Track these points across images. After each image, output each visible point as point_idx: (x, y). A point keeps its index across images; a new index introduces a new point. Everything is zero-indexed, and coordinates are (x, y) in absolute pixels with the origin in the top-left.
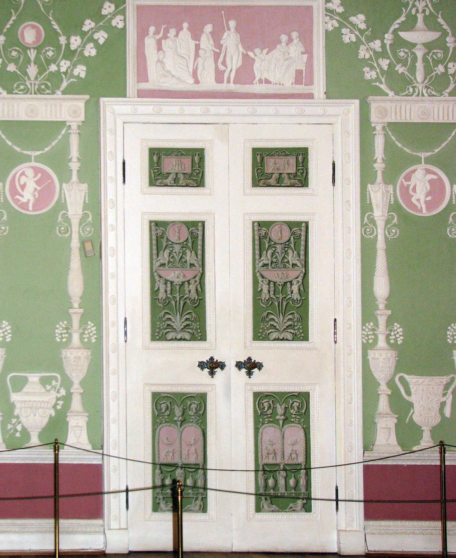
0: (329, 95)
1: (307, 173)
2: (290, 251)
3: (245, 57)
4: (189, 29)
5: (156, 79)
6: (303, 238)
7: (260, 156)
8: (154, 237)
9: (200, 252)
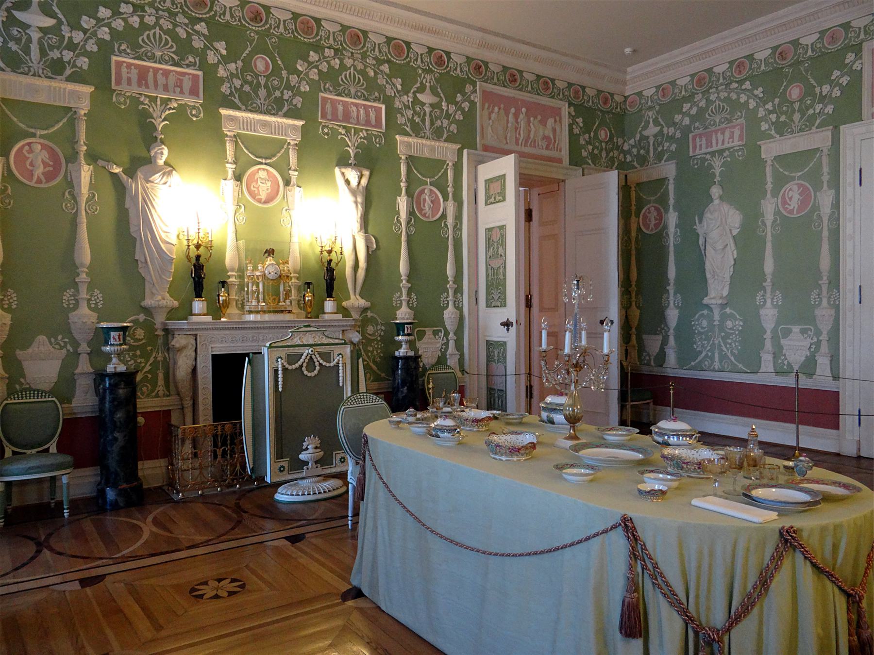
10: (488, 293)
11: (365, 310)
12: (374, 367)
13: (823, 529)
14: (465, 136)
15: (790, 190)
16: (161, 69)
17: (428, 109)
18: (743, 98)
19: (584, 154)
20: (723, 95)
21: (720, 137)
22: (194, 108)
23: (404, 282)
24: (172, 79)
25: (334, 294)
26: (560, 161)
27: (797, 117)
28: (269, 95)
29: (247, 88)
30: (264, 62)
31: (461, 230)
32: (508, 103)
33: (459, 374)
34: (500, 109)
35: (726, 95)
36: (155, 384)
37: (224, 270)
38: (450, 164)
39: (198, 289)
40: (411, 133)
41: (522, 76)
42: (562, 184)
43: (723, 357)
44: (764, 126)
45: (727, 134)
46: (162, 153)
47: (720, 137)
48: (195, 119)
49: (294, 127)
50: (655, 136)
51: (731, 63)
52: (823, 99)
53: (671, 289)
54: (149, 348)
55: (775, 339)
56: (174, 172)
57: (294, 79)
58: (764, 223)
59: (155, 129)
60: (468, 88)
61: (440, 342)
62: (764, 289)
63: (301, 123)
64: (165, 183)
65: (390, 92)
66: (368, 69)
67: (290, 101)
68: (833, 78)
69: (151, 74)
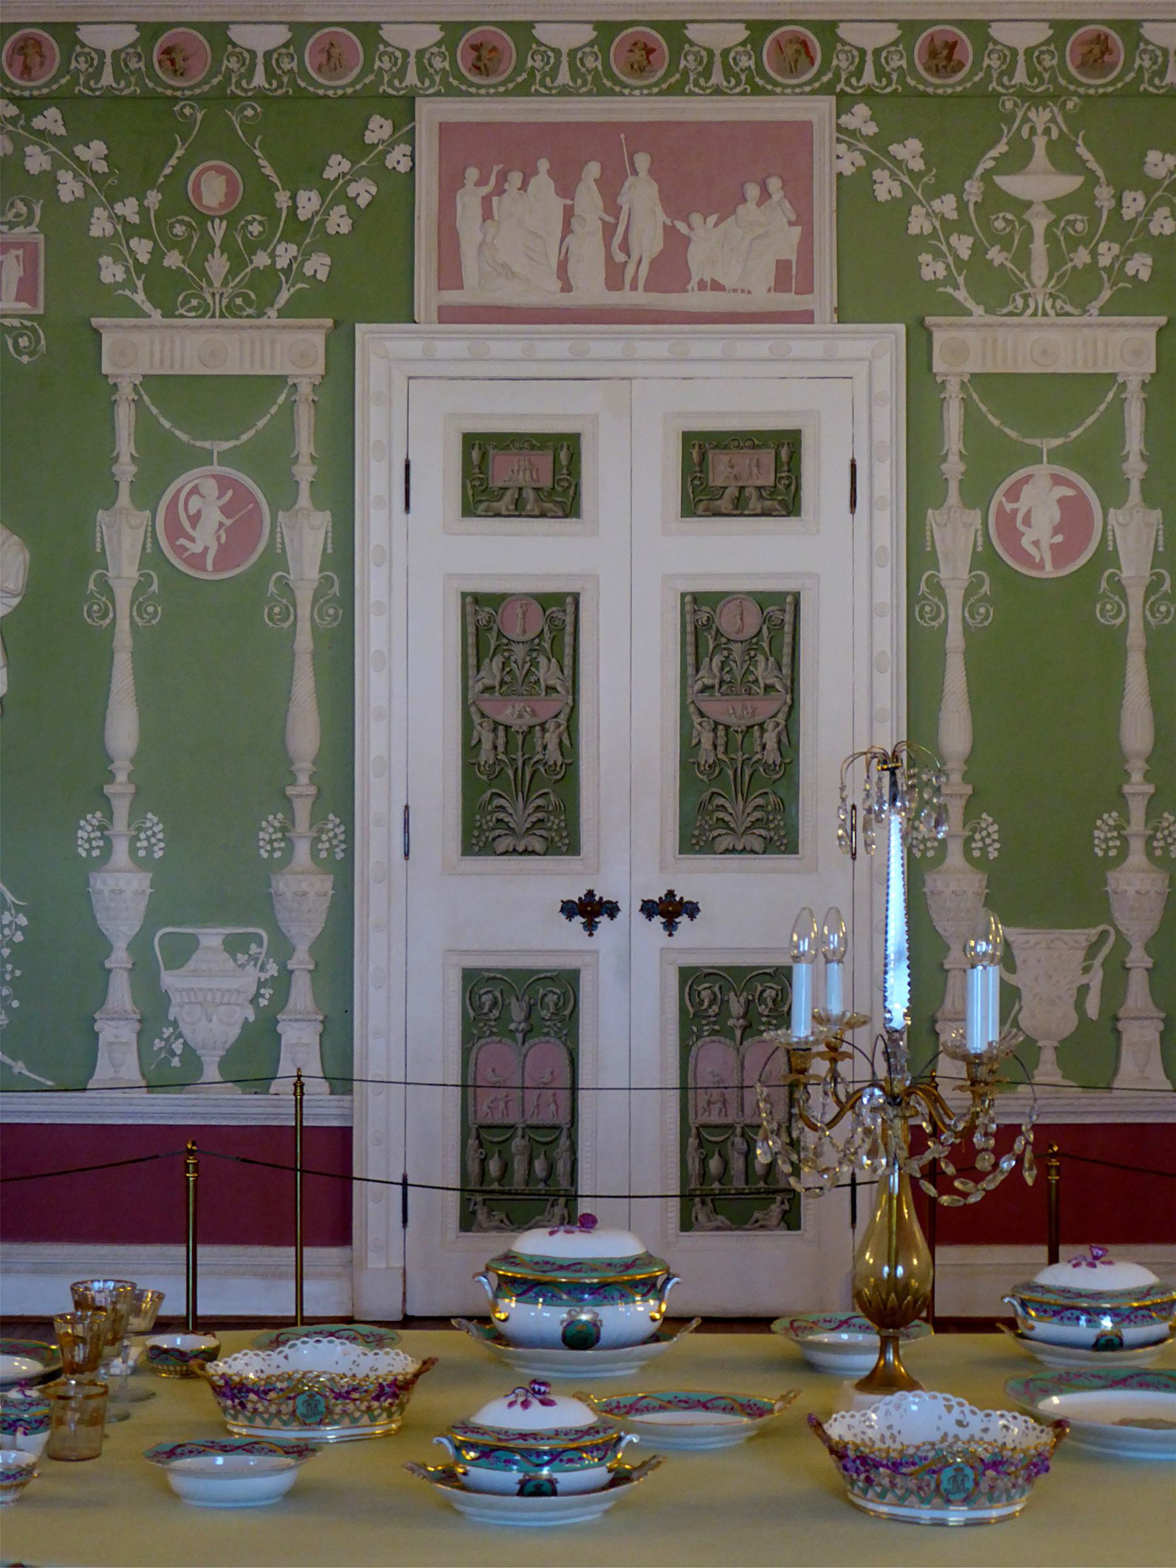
1: (798, 488)
3: (670, 232)
6: (788, 628)
8: (471, 629)
9: (568, 661)
15: (195, 490)
27: (218, 265)
44: (111, 271)
52: (297, 229)
58: (106, 588)
62: (105, 804)
68: (330, 174)
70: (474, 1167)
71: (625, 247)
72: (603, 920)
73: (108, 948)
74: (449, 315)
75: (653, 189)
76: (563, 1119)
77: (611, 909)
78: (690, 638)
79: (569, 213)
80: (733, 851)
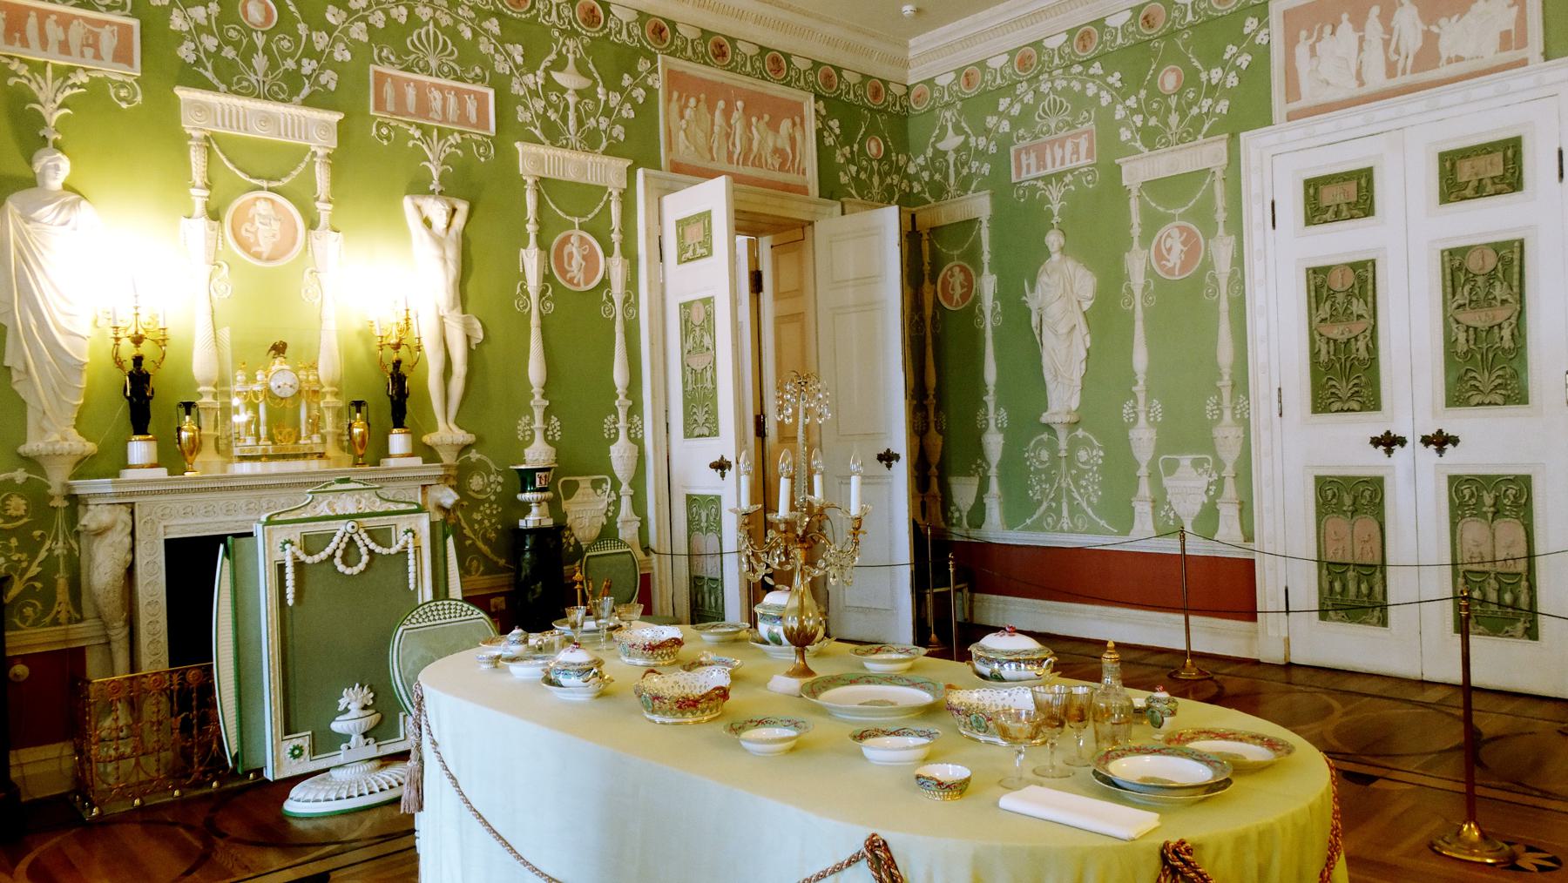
0: (1547, 56)
1: (1521, 173)
2: (1497, 284)
4: (1350, 20)
5: (1310, 94)
6: (1516, 263)
7: (1450, 162)
9: (1370, 299)
10: (688, 414)
11: (466, 448)
12: (485, 548)
13: (1241, 840)
14: (640, 147)
16: (53, 12)
17: (571, 99)
18: (1091, 90)
19: (844, 179)
20: (1060, 84)
21: (1058, 152)
22: (123, 85)
23: (537, 397)
24: (76, 33)
25: (407, 422)
26: (803, 190)
27: (1174, 119)
28: (273, 65)
29: (229, 52)
30: (261, 7)
31: (636, 305)
32: (712, 92)
33: (640, 555)
34: (698, 101)
35: (1065, 83)
36: (49, 597)
37: (193, 384)
38: (615, 193)
39: (140, 420)
40: (542, 138)
41: (734, 48)
42: (808, 228)
43: (1075, 510)
44: (1125, 135)
45: (1069, 146)
46: (57, 168)
47: (1058, 152)
48: (124, 106)
49: (325, 125)
50: (957, 151)
51: (1071, 32)
52: (1212, 90)
53: (990, 399)
54: (37, 533)
55: (1155, 477)
56: (83, 203)
57: (321, 40)
59: (42, 122)
60: (643, 65)
61: (602, 501)
62: (1134, 395)
63: (336, 117)
64: (64, 224)
65: (502, 67)
66: (461, 27)
67: (313, 77)
68: (1226, 57)
69: (32, 21)
70: (1326, 586)
71: (1397, 51)
72: (1397, 448)
73: (1138, 465)
74: (1291, 117)
75: (1414, 11)
76: (1377, 561)
77: (1402, 441)
78: (1448, 277)
79: (1362, 40)
80: (1482, 404)
